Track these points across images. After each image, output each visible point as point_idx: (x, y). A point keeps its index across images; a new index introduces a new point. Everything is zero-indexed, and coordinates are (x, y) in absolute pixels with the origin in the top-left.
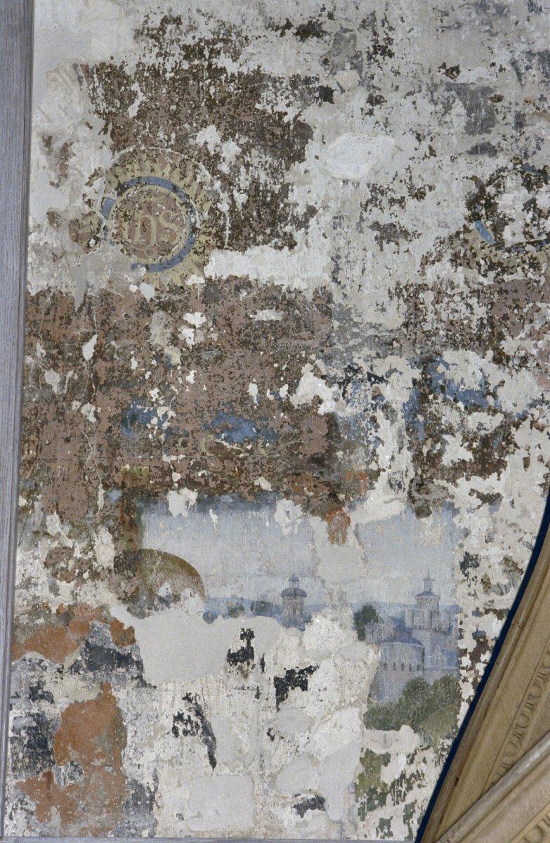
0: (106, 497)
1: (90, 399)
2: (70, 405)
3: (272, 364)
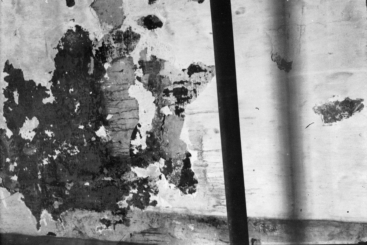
0: (107, 176)
1: (63, 185)
2: (67, 195)
3: (37, 91)
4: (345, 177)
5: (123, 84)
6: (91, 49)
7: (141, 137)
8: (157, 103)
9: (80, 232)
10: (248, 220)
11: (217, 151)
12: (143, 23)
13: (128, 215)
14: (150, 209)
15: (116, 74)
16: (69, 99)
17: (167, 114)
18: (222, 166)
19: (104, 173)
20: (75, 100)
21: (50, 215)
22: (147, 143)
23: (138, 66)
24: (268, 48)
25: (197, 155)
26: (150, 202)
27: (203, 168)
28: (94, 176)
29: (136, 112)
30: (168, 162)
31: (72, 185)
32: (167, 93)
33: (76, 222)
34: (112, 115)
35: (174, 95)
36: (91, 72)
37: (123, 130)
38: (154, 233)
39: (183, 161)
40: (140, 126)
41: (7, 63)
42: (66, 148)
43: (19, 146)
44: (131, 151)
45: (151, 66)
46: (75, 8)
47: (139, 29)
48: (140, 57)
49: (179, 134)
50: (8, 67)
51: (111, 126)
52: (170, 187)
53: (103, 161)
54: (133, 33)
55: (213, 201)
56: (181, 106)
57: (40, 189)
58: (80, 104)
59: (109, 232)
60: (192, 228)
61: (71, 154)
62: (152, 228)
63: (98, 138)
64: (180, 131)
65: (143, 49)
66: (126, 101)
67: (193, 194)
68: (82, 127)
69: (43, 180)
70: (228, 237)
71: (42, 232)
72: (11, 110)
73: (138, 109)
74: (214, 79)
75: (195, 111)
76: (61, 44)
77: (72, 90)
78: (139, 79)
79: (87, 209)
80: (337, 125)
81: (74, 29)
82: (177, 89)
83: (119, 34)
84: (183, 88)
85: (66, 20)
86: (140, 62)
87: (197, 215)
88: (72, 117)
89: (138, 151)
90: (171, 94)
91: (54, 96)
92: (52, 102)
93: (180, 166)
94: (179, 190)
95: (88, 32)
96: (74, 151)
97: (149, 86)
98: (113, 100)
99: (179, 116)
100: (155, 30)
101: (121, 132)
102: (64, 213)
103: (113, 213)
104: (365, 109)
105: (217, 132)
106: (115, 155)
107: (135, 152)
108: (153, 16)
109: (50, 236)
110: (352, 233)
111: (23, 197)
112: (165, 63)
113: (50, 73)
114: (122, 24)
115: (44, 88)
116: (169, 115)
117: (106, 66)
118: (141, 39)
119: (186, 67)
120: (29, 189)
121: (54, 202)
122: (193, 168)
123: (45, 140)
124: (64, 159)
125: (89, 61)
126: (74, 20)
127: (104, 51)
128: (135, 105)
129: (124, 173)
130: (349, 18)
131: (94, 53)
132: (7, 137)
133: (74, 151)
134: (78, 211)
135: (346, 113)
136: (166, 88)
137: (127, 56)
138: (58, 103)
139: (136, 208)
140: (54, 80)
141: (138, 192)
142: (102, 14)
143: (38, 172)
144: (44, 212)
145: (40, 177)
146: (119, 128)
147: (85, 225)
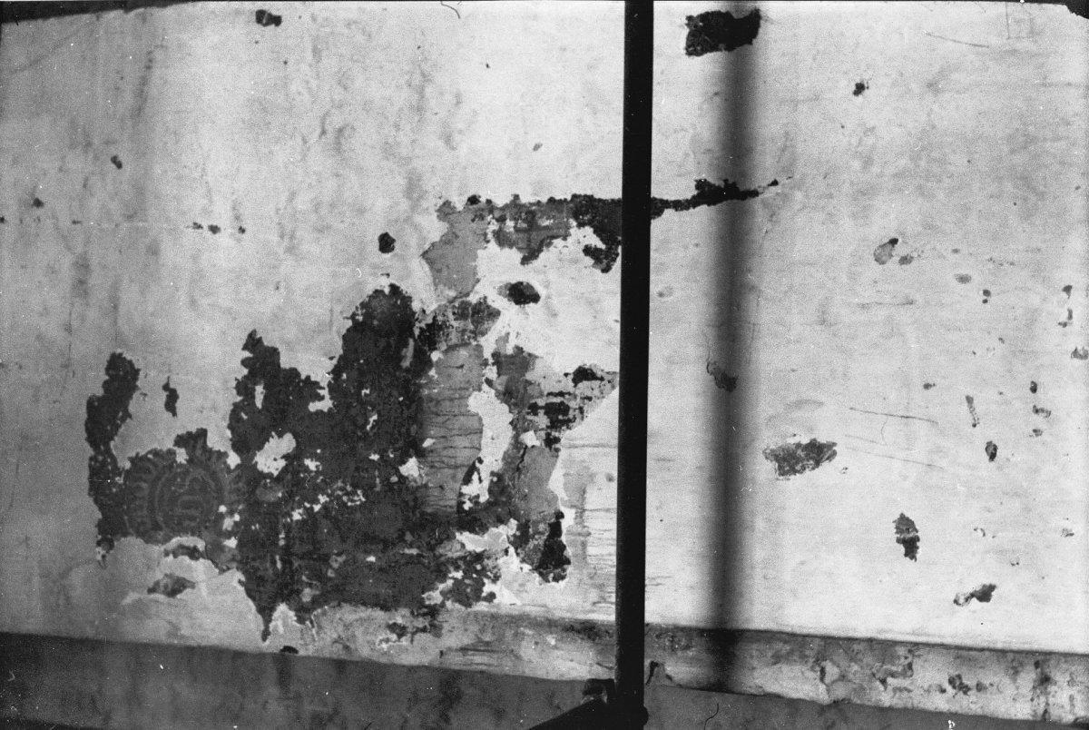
0: (411, 546)
1: (325, 559)
2: (330, 579)
4: (802, 563)
5: (461, 389)
6: (411, 326)
7: (480, 481)
8: (516, 425)
9: (346, 648)
10: (646, 629)
11: (608, 510)
12: (508, 292)
13: (440, 618)
14: (482, 607)
15: (450, 370)
16: (359, 407)
17: (530, 444)
18: (615, 536)
19: (405, 541)
20: (370, 408)
21: (292, 614)
22: (490, 491)
23: (491, 361)
24: (701, 351)
25: (574, 516)
26: (484, 594)
27: (582, 539)
28: (387, 544)
29: (475, 437)
30: (523, 527)
31: (341, 559)
32: (534, 409)
33: (340, 628)
34: (434, 440)
35: (545, 413)
36: (406, 363)
37: (449, 467)
38: (483, 651)
39: (550, 525)
40: (481, 461)
41: (252, 336)
42: (340, 493)
43: (248, 484)
44: (461, 504)
45: (513, 364)
46: (396, 255)
47: (499, 302)
48: (495, 346)
49: (548, 479)
50: (253, 342)
51: (429, 459)
52: (521, 569)
53: (407, 520)
54: (488, 307)
55: (593, 595)
56: (555, 434)
57: (279, 565)
58: (378, 416)
59: (400, 646)
60: (553, 642)
61: (349, 504)
62: (480, 641)
63: (403, 479)
64: (550, 474)
65: (503, 334)
66: (462, 418)
67: (560, 582)
68: (375, 457)
69: (287, 548)
70: (614, 659)
71: (272, 645)
72: (245, 417)
73: (481, 432)
74: (616, 393)
75: (577, 442)
76: (360, 312)
77: (368, 392)
78: (489, 382)
79: (364, 604)
80: (796, 480)
81: (387, 290)
82: (552, 404)
83: (465, 305)
84: (562, 403)
85: (374, 274)
86: (496, 355)
87: (564, 618)
88: (360, 438)
89: (471, 505)
90: (541, 412)
91: (331, 399)
92: (326, 410)
93: (542, 533)
94: (536, 575)
95: (411, 298)
96: (356, 498)
97: (504, 394)
98: (438, 415)
99: (550, 448)
100: (526, 305)
101: (446, 470)
102: (319, 611)
103: (412, 613)
104: (837, 458)
105: (610, 479)
106: (429, 510)
107: (467, 506)
108: (525, 284)
109: (287, 653)
110: (807, 653)
111: (243, 579)
112: (537, 361)
113: (331, 358)
114: (471, 291)
115: (316, 384)
116: (533, 447)
117: (435, 356)
118: (501, 318)
119: (571, 370)
120: (257, 564)
121: (302, 591)
122: (564, 539)
123: (302, 475)
124: (334, 513)
125: (406, 345)
126: (388, 275)
127: (434, 332)
128: (476, 425)
129: (441, 542)
130: (823, 322)
131: (417, 332)
132: (228, 467)
133: (356, 498)
134: (347, 607)
135: (812, 462)
136: (534, 401)
137: (474, 343)
138: (338, 412)
139: (457, 605)
140: (336, 372)
141: (464, 578)
142: (439, 271)
143: (280, 533)
144: (282, 608)
145: (282, 543)
146: (443, 462)
147: (356, 633)
